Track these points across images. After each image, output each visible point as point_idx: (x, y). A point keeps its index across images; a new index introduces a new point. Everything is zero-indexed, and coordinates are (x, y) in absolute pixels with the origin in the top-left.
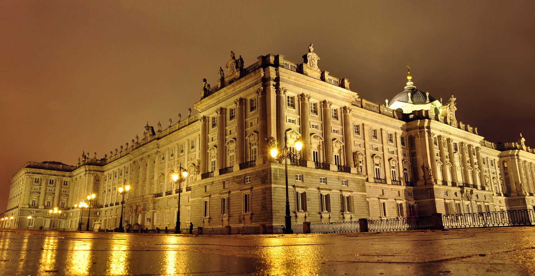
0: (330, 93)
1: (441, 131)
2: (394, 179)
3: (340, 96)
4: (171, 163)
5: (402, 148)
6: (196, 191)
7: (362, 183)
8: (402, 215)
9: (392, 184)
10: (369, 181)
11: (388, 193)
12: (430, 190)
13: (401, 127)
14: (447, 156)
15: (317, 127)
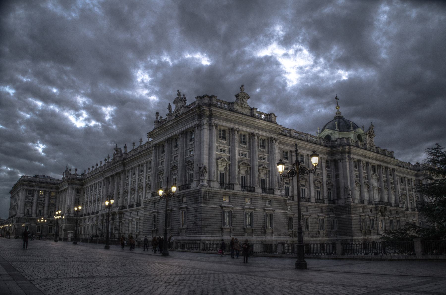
0: (258, 126)
1: (360, 156)
2: (319, 198)
3: (267, 128)
4: (133, 181)
5: (327, 171)
6: (147, 206)
7: (284, 202)
8: (323, 229)
9: (316, 202)
10: (295, 200)
11: (312, 210)
12: (348, 207)
13: (326, 153)
14: (365, 177)
15: (245, 155)
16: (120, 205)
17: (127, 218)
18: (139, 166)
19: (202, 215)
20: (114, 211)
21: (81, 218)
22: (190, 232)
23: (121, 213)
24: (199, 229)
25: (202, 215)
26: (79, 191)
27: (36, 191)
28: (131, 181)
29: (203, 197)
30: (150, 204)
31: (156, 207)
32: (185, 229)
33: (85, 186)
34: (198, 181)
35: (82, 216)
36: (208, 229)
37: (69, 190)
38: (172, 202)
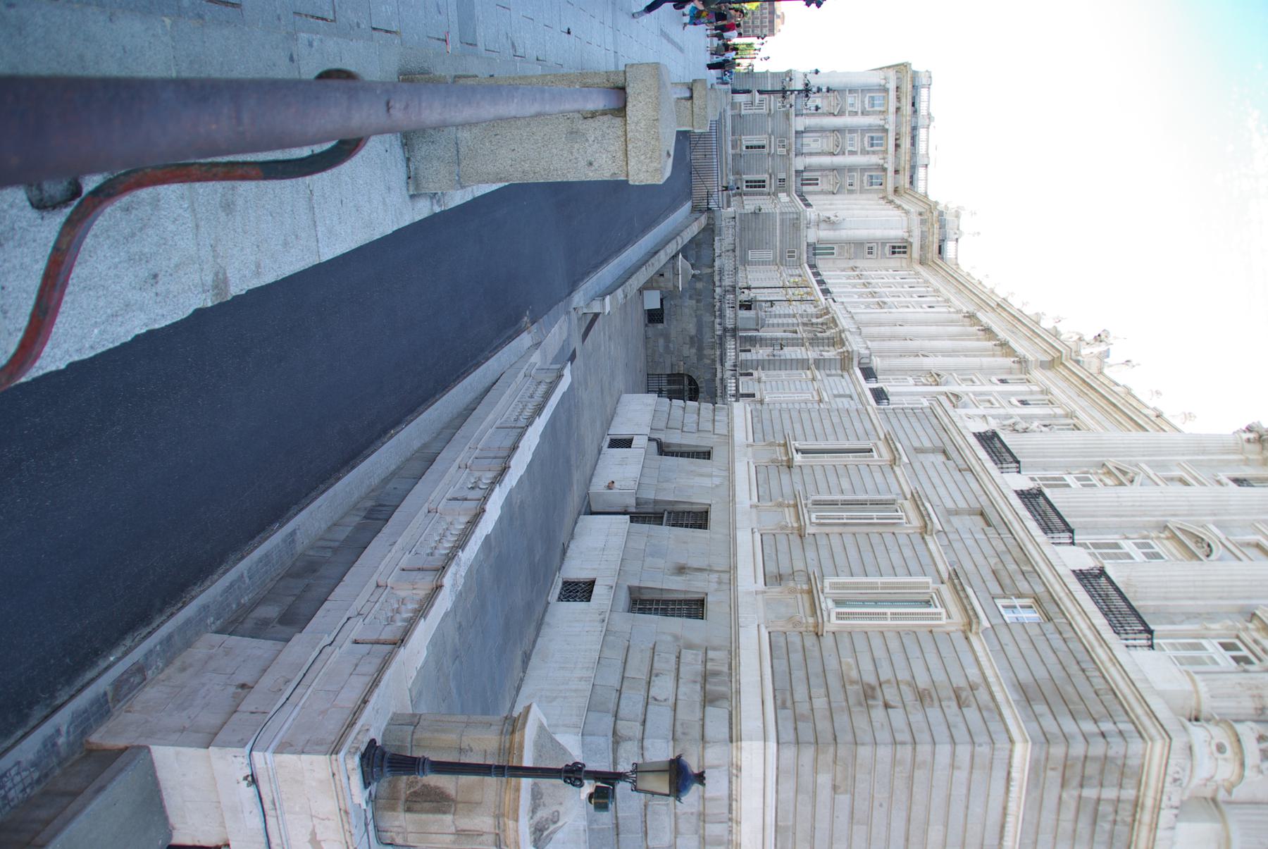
16: (877, 363)
17: (828, 388)
18: (1070, 415)
19: (944, 750)
20: (849, 337)
21: (806, 265)
22: (797, 657)
23: (845, 362)
24: (823, 725)
25: (944, 750)
26: (899, 253)
27: (882, 123)
28: (990, 394)
29: (1095, 759)
30: (931, 431)
31: (921, 456)
32: (814, 613)
33: (919, 268)
34: (1198, 710)
35: (812, 266)
36: (825, 794)
37: (901, 217)
38: (980, 536)
